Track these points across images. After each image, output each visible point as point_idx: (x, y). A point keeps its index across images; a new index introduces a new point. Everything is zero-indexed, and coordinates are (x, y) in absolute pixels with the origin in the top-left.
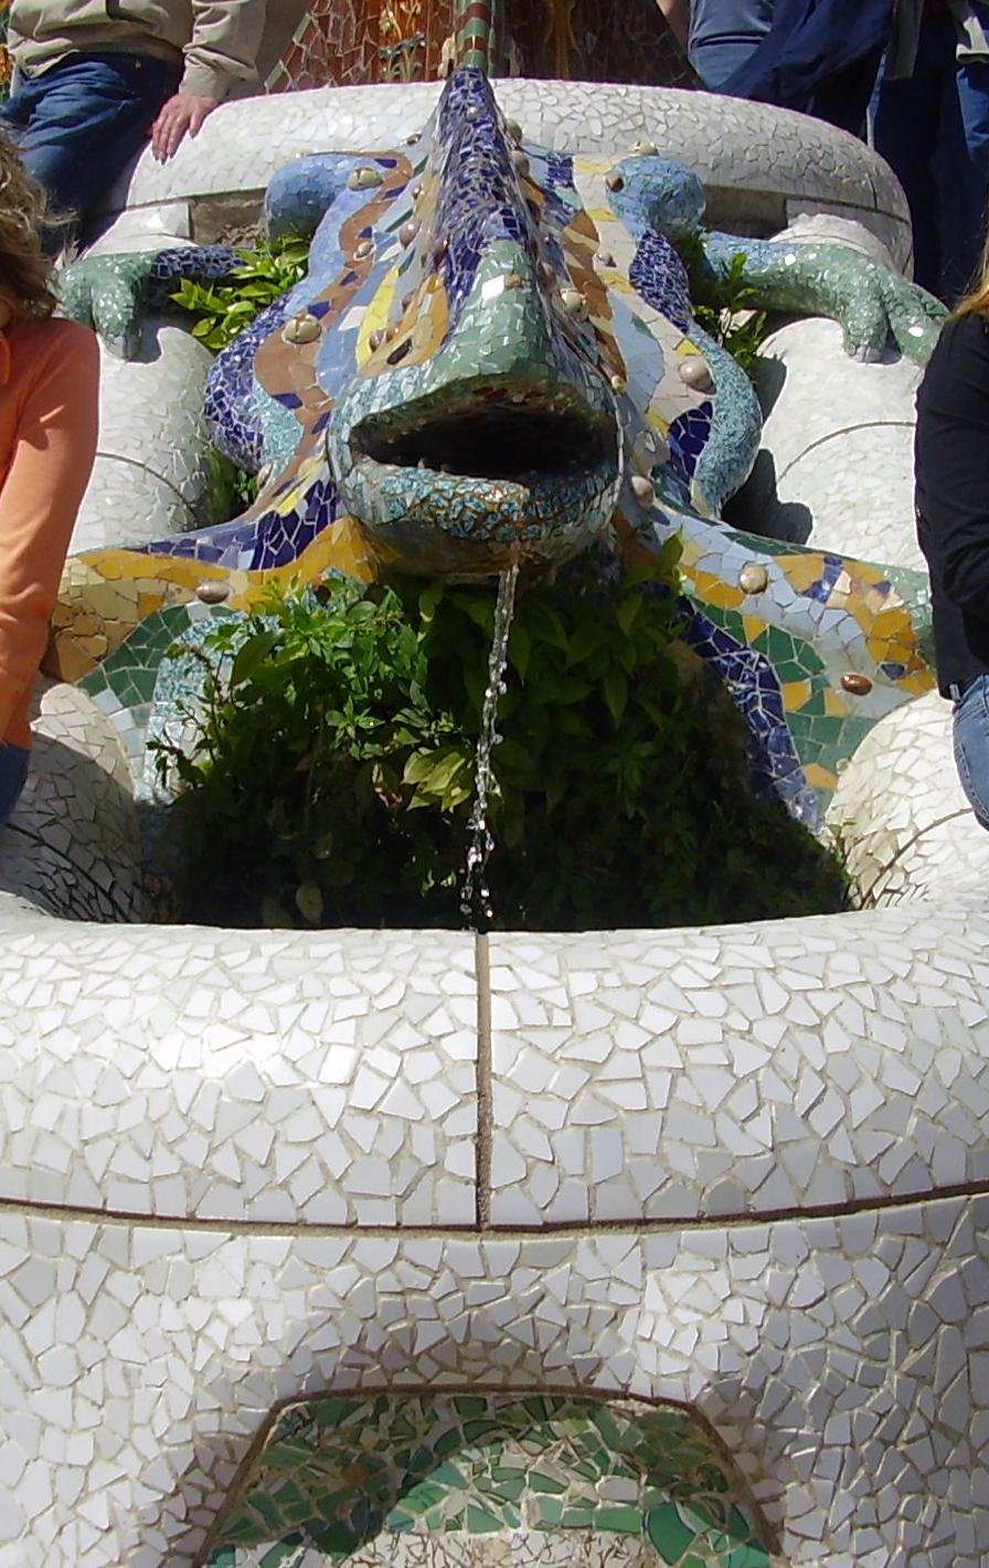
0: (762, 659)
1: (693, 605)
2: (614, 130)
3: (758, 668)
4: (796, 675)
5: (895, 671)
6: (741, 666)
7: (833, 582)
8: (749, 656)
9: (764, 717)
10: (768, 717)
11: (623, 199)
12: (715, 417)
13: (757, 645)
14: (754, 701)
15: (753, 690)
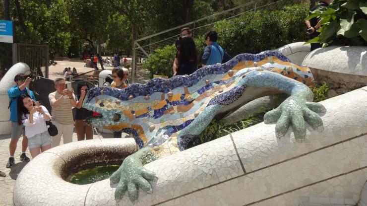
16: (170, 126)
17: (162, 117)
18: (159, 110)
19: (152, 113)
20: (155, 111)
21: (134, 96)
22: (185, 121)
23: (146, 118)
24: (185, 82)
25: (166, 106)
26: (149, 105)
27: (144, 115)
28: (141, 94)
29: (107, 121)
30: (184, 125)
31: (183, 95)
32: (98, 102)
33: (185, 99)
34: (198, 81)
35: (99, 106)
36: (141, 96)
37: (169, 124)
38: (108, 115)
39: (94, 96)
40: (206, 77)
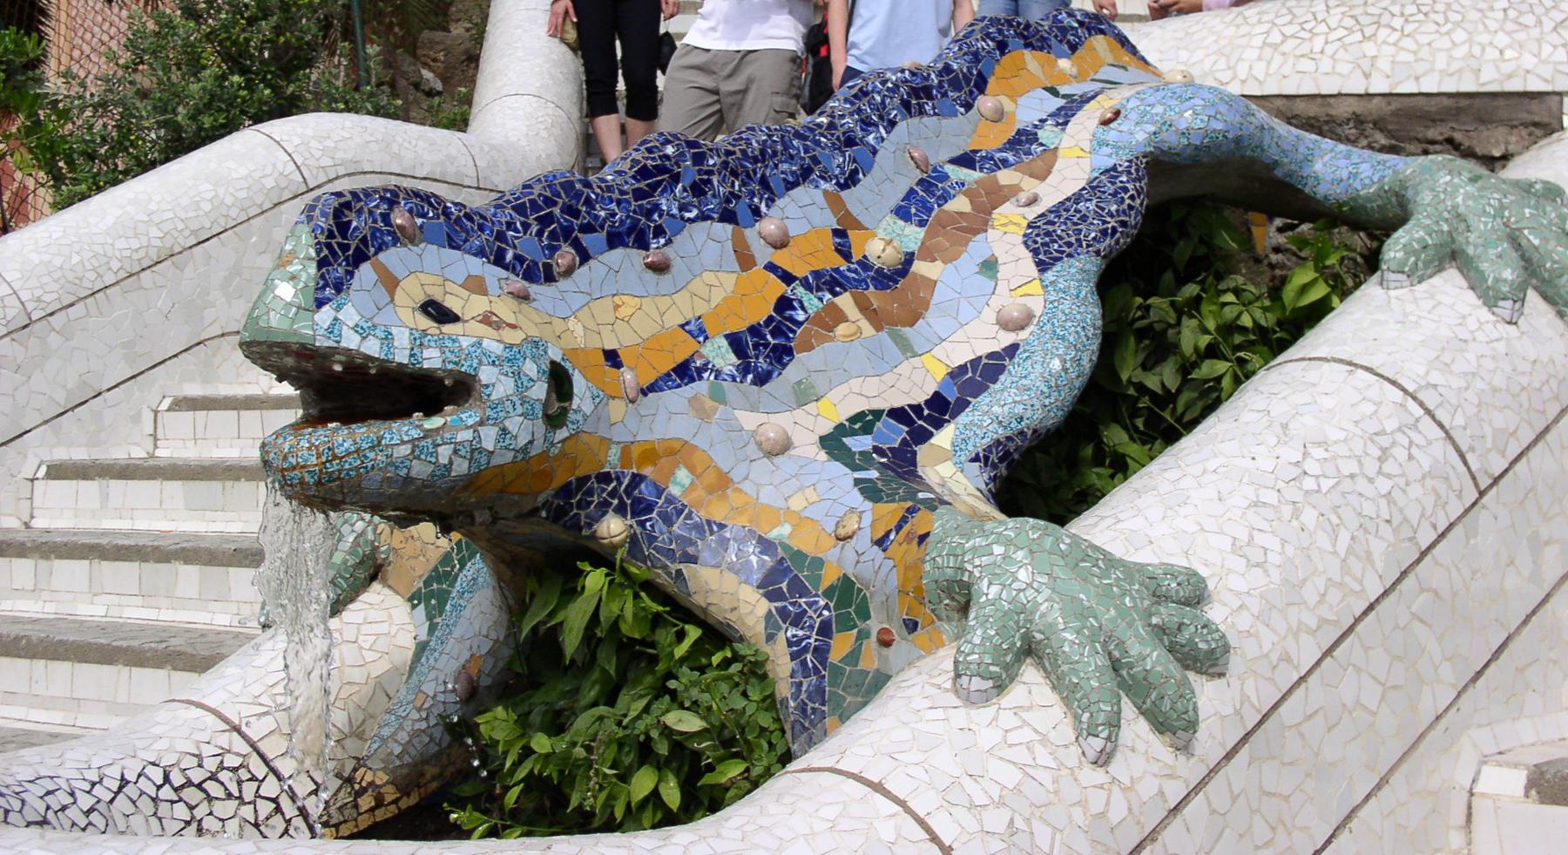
0: (827, 607)
1: (779, 549)
2: (1338, 44)
3: (821, 615)
4: (847, 625)
5: (912, 626)
6: (805, 612)
7: (899, 528)
8: (817, 602)
9: (810, 665)
10: (814, 665)
11: (1112, 134)
12: (1016, 360)
13: (828, 593)
14: (805, 649)
15: (809, 637)
16: (877, 414)
17: (793, 372)
18: (754, 330)
19: (720, 355)
20: (735, 342)
21: (585, 257)
22: (941, 373)
23: (701, 387)
24: (816, 161)
25: (784, 304)
26: (682, 308)
27: (685, 372)
28: (614, 241)
29: (513, 424)
30: (952, 396)
31: (836, 233)
32: (399, 295)
33: (856, 257)
34: (875, 152)
35: (425, 323)
36: (618, 253)
37: (864, 406)
38: (517, 375)
39: (360, 258)
40: (902, 126)
